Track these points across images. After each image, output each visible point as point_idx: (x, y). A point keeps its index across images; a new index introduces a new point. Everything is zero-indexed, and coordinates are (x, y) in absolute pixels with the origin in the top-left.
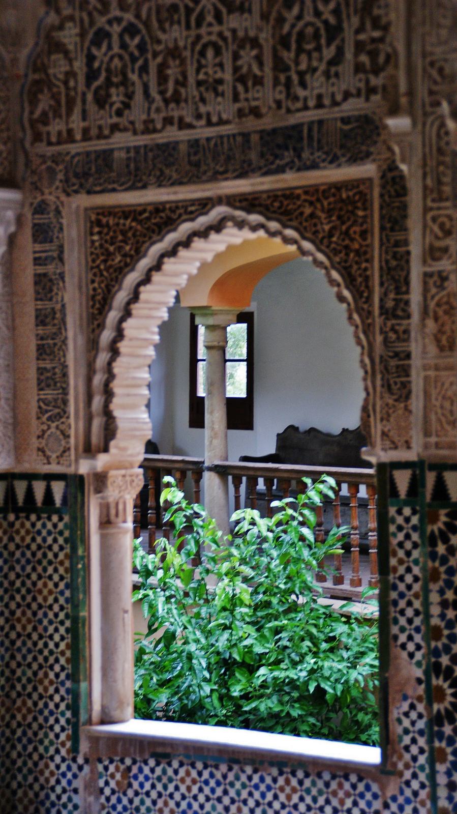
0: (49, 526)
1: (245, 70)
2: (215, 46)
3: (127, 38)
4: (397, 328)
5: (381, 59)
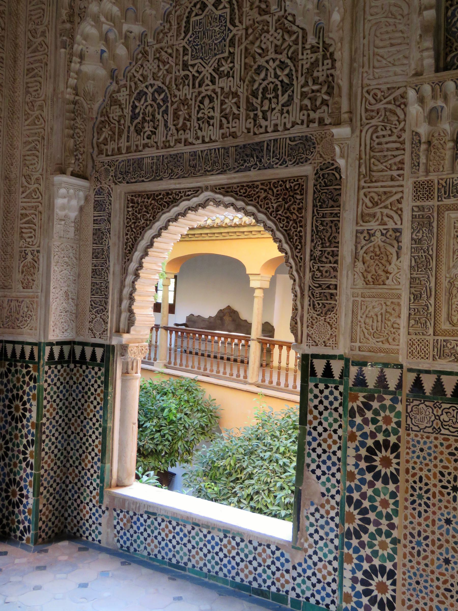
0: (93, 373)
1: (228, 111)
2: (210, 97)
3: (156, 95)
4: (321, 269)
5: (318, 103)
